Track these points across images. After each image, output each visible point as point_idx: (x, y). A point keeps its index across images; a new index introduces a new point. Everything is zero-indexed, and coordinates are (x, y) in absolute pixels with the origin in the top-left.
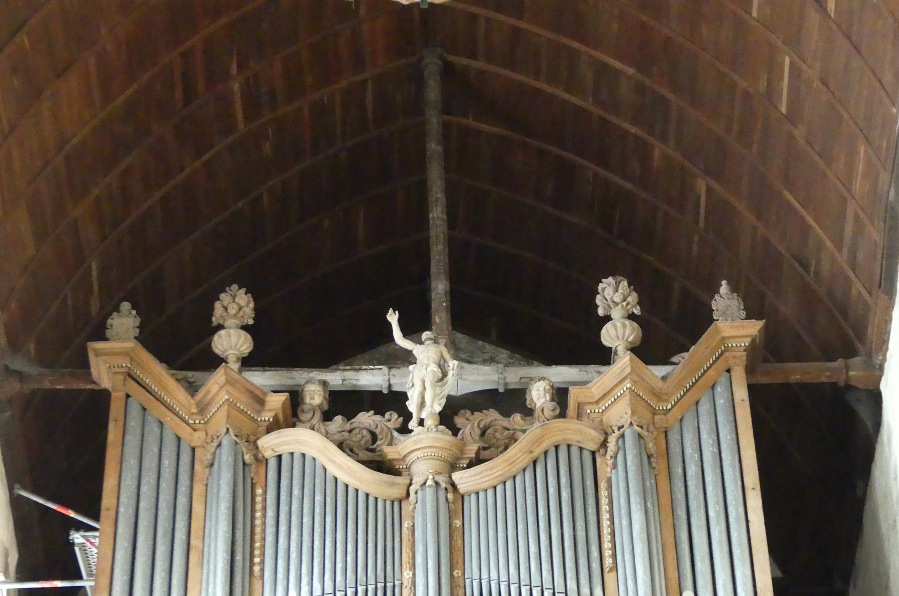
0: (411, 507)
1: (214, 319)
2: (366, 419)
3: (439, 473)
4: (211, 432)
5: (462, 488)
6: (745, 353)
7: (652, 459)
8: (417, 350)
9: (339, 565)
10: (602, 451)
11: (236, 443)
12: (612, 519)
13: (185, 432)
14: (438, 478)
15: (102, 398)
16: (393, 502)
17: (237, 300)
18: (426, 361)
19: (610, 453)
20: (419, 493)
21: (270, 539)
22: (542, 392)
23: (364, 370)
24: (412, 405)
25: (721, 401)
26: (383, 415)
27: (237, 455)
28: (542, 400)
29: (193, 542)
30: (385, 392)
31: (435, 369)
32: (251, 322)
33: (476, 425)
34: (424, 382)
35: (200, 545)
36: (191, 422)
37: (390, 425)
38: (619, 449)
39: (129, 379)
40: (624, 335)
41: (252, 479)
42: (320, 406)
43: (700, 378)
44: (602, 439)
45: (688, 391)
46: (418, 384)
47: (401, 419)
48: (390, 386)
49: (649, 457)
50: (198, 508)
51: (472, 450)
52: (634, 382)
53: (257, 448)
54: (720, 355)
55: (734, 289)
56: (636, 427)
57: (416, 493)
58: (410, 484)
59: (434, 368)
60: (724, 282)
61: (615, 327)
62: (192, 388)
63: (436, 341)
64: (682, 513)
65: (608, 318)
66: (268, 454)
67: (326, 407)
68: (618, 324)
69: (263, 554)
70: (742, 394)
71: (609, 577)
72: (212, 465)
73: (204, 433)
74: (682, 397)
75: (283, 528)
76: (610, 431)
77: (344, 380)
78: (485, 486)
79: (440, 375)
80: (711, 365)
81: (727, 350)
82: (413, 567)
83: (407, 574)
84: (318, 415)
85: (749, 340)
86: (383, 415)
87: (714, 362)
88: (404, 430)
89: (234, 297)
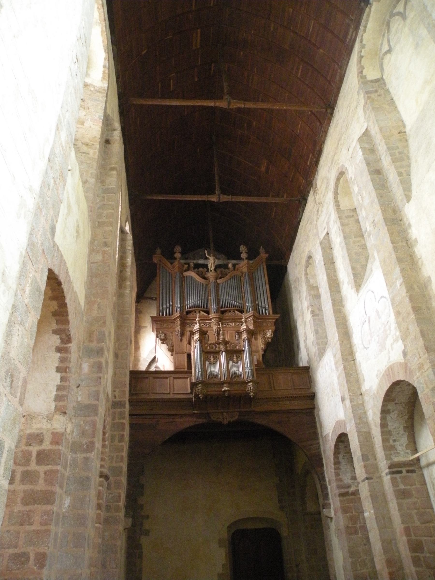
2: (201, 269)
8: (210, 258)
13: (170, 271)
15: (155, 264)
24: (209, 268)
25: (261, 268)
27: (180, 276)
32: (180, 251)
46: (210, 263)
50: (173, 285)
51: (220, 276)
55: (263, 247)
59: (213, 261)
62: (171, 263)
63: (213, 256)
65: (242, 253)
66: (185, 276)
70: (265, 267)
71: (244, 299)
72: (175, 277)
82: (211, 296)
83: (210, 298)
84: (193, 269)
88: (208, 271)
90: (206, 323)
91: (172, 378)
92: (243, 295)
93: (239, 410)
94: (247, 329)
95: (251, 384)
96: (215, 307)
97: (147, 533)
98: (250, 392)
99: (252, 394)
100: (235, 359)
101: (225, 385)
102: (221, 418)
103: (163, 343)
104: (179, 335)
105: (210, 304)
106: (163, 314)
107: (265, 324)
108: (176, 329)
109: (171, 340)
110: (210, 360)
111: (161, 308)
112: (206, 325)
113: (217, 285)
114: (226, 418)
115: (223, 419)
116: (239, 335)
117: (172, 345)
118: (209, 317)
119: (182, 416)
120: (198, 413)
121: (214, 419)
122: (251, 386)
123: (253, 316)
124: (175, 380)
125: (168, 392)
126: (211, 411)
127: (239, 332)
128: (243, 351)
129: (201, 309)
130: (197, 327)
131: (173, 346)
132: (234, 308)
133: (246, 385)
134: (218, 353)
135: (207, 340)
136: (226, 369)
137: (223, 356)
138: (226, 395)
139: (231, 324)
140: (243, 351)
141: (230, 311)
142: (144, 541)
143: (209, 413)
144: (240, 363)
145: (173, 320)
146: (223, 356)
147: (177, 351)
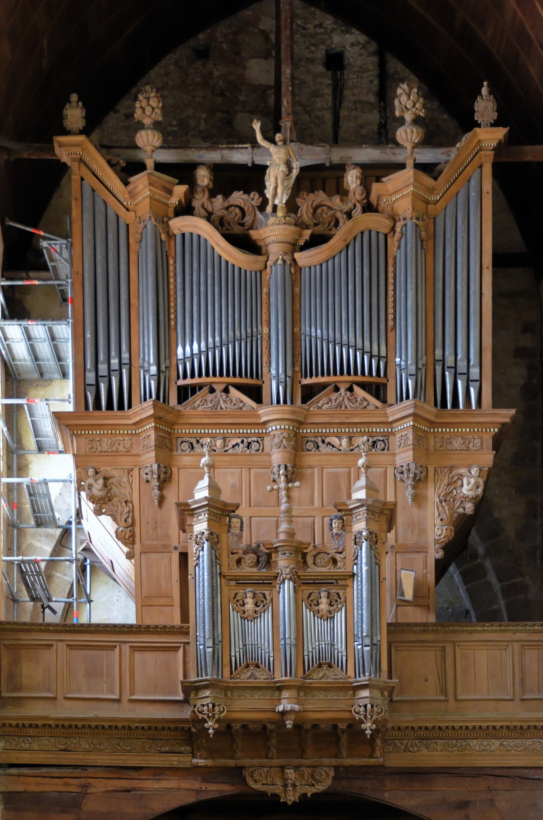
0: (268, 277)
1: (135, 116)
3: (286, 254)
4: (139, 214)
5: (300, 263)
6: (493, 152)
7: (424, 243)
8: (272, 148)
9: (224, 325)
10: (391, 234)
11: (156, 225)
12: (395, 290)
13: (122, 211)
14: (285, 257)
15: (63, 168)
16: (256, 272)
17: (151, 102)
18: (278, 161)
19: (397, 235)
20: (273, 268)
21: (179, 300)
22: (354, 179)
23: (236, 148)
24: (269, 193)
26: (249, 194)
27: (156, 235)
28: (355, 185)
29: (132, 301)
30: (250, 165)
31: (284, 169)
33: (310, 204)
34: (276, 179)
35: (137, 303)
36: (125, 203)
37: (254, 203)
38: (402, 234)
39: (82, 165)
40: (412, 139)
41: (167, 252)
42: (207, 186)
43: (461, 173)
44: (392, 225)
45: (452, 184)
47: (261, 199)
48: (253, 161)
49: (422, 241)
52: (415, 187)
53: (169, 226)
54: (476, 154)
56: (415, 220)
57: (271, 267)
58: (267, 260)
60: (485, 83)
61: (406, 132)
64: (440, 285)
65: (401, 121)
66: (176, 232)
67: (211, 186)
68: (409, 131)
69: (176, 311)
71: (391, 335)
72: (141, 240)
73: (134, 213)
74: (447, 189)
75: (188, 293)
76: (397, 219)
77: (222, 157)
78: (314, 264)
79: (287, 173)
80: (469, 162)
81: (481, 150)
84: (207, 194)
85: (497, 141)
86: (249, 194)
87: (472, 159)
88: (262, 208)
89: (148, 99)
90: (248, 436)
91: (126, 648)
92: (391, 317)
93: (334, 761)
94: (370, 502)
95: (365, 693)
96: (282, 377)
98: (362, 717)
99: (368, 726)
100: (324, 606)
101: (285, 694)
102: (279, 782)
103: (98, 512)
104: (155, 483)
105: (265, 359)
106: (97, 406)
107: (457, 443)
108: (144, 458)
109: (126, 502)
110: (244, 605)
111: (91, 377)
112: (249, 445)
114: (294, 786)
115: (285, 786)
116: (341, 518)
117: (130, 520)
118: (259, 416)
120: (206, 767)
121: (254, 786)
122: (367, 701)
123: (414, 415)
124: (138, 656)
125: (116, 697)
126: (247, 762)
127: (345, 510)
128: (353, 575)
129: (231, 380)
131: (133, 524)
132: (352, 378)
133: (354, 695)
135: (237, 535)
136: (294, 642)
138: (289, 724)
139: (335, 441)
140: (353, 575)
141: (337, 389)
143: (240, 769)
144: (340, 617)
145: (135, 424)
147: (146, 542)
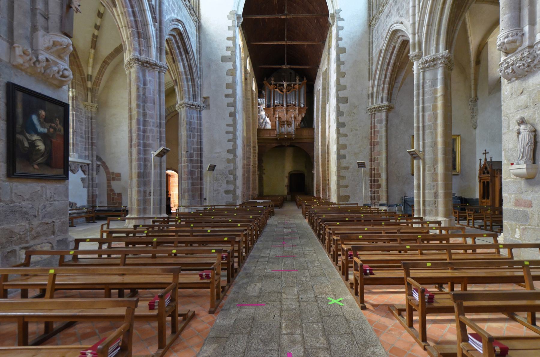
15: (264, 84)
97: (265, 174)
113: (287, 94)
119: (274, 143)
130: (278, 116)
134: (284, 124)
137: (286, 125)
142: (264, 176)
146: (286, 125)
